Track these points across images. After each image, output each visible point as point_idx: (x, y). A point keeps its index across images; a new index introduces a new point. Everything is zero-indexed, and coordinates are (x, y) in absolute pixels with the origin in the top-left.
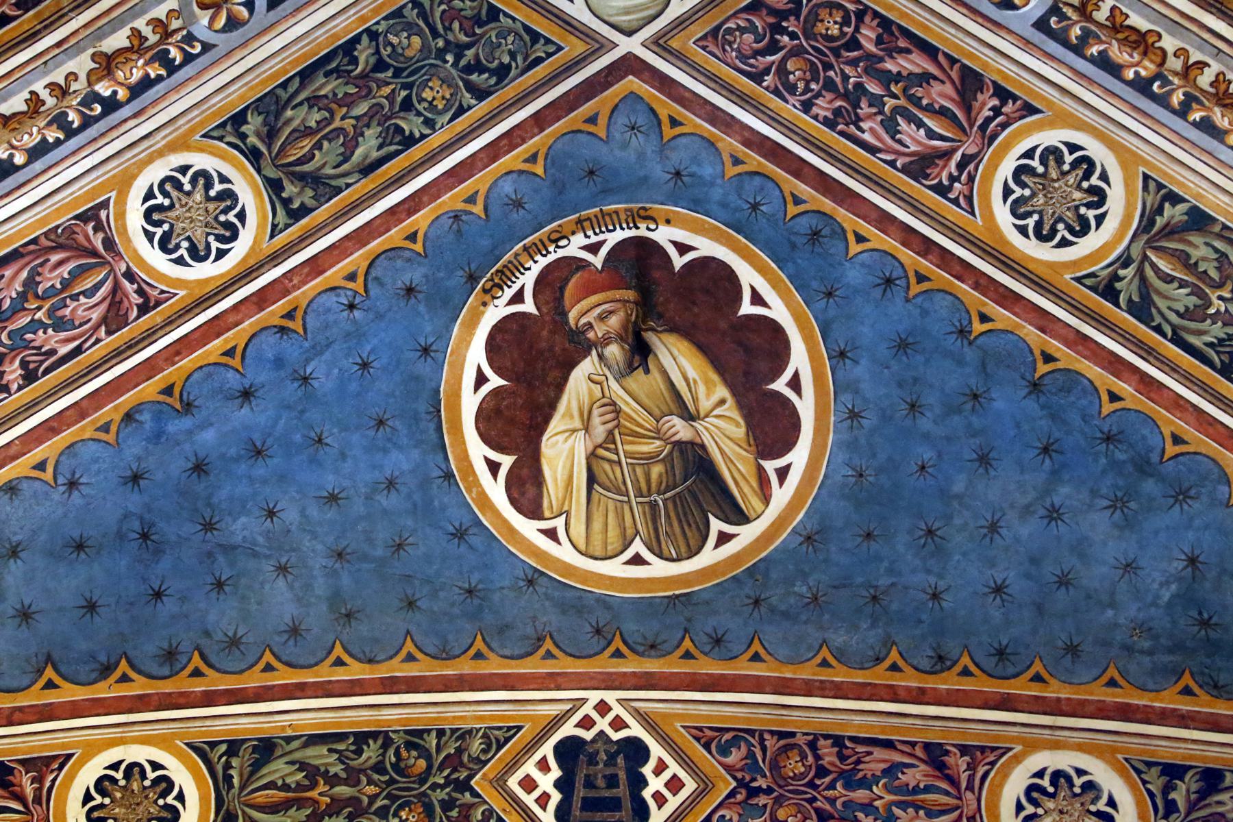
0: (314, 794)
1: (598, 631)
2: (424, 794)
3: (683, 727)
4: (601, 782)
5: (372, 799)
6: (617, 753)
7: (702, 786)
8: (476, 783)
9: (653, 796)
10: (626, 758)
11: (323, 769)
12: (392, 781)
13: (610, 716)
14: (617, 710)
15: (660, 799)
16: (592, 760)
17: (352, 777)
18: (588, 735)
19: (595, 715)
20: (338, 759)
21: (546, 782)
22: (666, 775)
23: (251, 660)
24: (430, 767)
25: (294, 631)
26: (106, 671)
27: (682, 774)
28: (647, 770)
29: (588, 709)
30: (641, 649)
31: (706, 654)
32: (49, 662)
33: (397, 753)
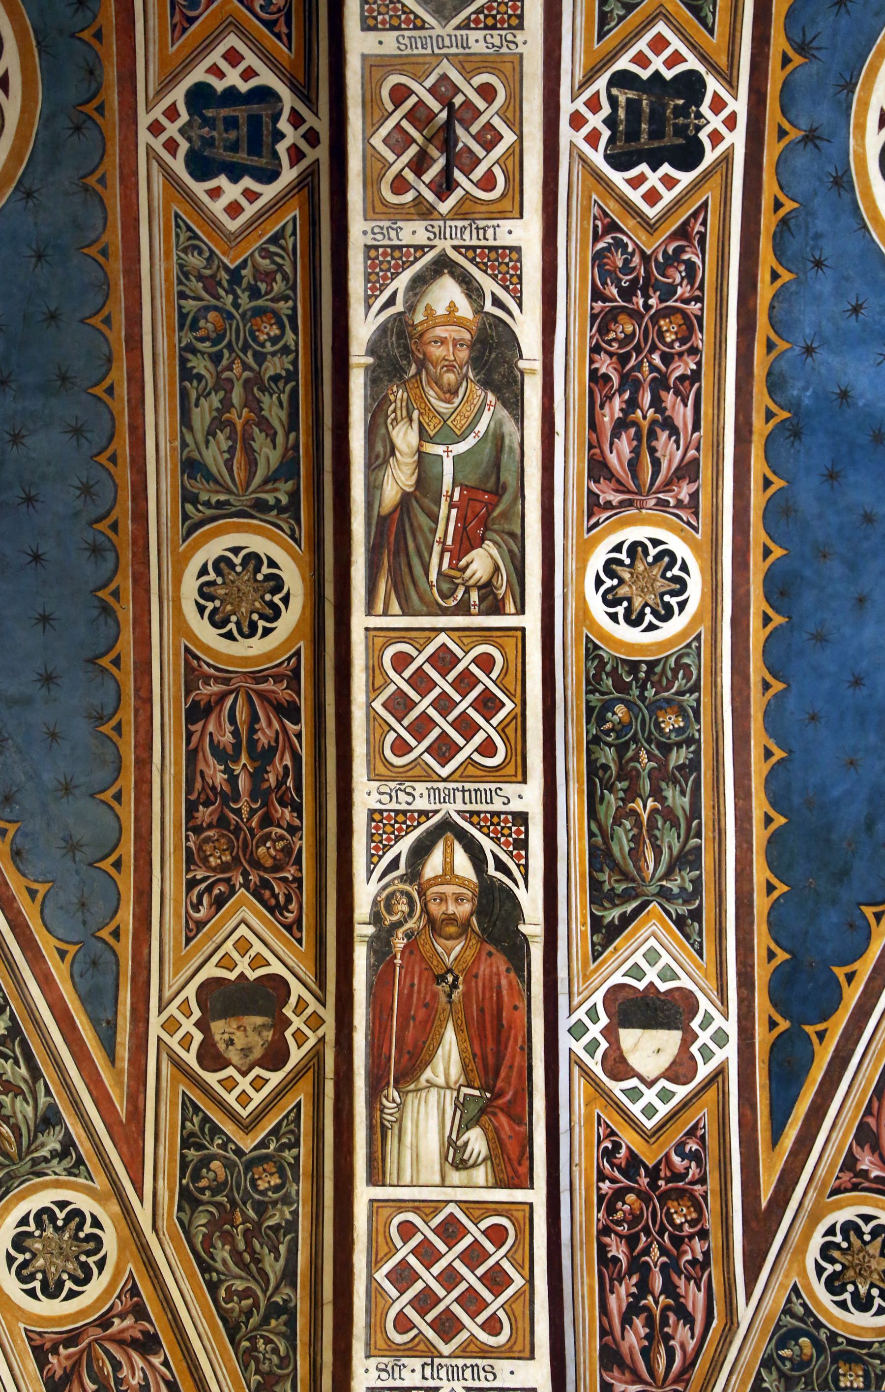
0: (239, 424)
1: (78, 129)
2: (243, 316)
3: (173, 44)
4: (233, 135)
5: (246, 367)
6: (202, 116)
7: (232, 28)
8: (232, 261)
9: (246, 81)
10: (207, 107)
11: (215, 414)
12: (229, 346)
13: (164, 121)
14: (157, 113)
15: (249, 74)
16: (209, 142)
17: (223, 385)
18: (184, 146)
19: (163, 137)
20: (205, 397)
21: (232, 191)
22: (224, 65)
23: (104, 475)
24: (216, 308)
25: (77, 432)
26: (106, 610)
27: (222, 48)
28: (220, 86)
29: (157, 144)
30: (94, 86)
31: (95, 17)
32: (95, 661)
33: (202, 340)
